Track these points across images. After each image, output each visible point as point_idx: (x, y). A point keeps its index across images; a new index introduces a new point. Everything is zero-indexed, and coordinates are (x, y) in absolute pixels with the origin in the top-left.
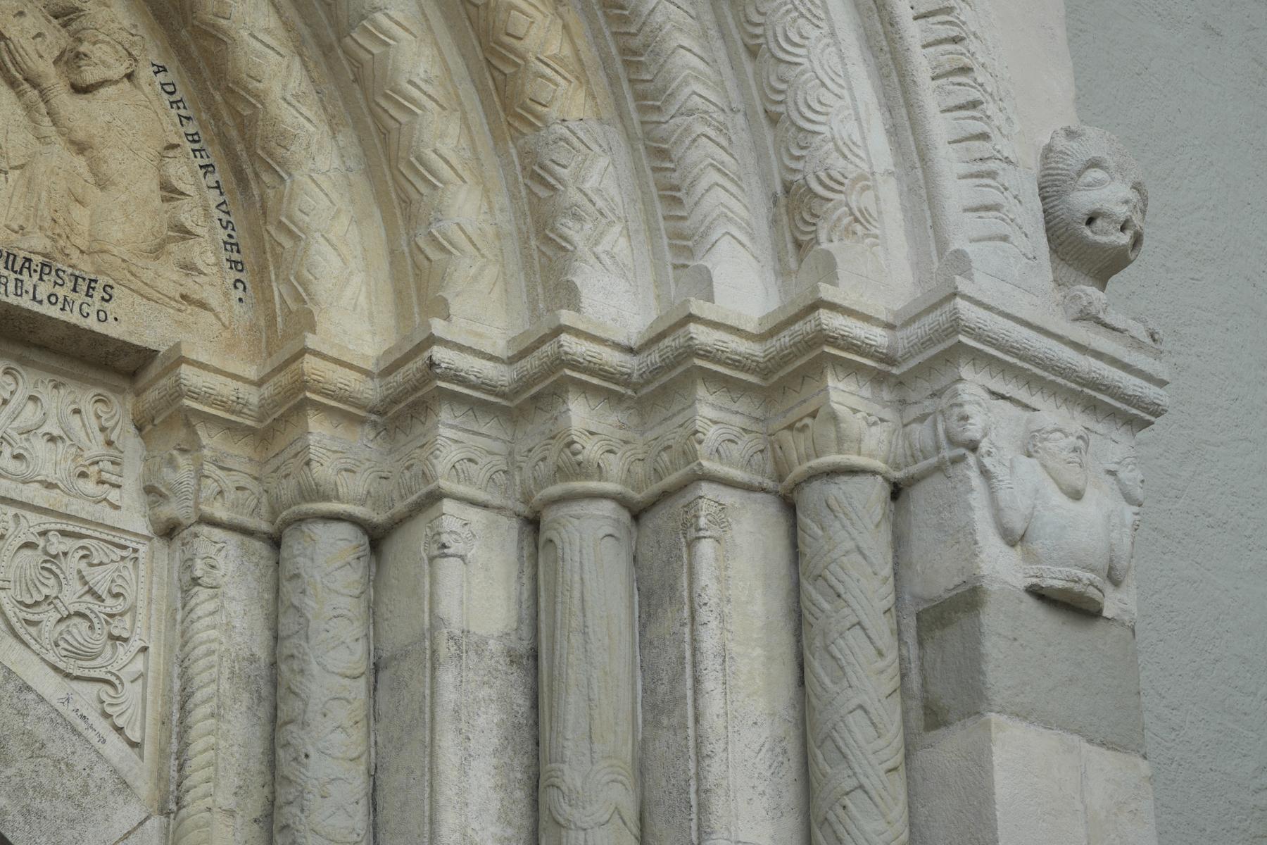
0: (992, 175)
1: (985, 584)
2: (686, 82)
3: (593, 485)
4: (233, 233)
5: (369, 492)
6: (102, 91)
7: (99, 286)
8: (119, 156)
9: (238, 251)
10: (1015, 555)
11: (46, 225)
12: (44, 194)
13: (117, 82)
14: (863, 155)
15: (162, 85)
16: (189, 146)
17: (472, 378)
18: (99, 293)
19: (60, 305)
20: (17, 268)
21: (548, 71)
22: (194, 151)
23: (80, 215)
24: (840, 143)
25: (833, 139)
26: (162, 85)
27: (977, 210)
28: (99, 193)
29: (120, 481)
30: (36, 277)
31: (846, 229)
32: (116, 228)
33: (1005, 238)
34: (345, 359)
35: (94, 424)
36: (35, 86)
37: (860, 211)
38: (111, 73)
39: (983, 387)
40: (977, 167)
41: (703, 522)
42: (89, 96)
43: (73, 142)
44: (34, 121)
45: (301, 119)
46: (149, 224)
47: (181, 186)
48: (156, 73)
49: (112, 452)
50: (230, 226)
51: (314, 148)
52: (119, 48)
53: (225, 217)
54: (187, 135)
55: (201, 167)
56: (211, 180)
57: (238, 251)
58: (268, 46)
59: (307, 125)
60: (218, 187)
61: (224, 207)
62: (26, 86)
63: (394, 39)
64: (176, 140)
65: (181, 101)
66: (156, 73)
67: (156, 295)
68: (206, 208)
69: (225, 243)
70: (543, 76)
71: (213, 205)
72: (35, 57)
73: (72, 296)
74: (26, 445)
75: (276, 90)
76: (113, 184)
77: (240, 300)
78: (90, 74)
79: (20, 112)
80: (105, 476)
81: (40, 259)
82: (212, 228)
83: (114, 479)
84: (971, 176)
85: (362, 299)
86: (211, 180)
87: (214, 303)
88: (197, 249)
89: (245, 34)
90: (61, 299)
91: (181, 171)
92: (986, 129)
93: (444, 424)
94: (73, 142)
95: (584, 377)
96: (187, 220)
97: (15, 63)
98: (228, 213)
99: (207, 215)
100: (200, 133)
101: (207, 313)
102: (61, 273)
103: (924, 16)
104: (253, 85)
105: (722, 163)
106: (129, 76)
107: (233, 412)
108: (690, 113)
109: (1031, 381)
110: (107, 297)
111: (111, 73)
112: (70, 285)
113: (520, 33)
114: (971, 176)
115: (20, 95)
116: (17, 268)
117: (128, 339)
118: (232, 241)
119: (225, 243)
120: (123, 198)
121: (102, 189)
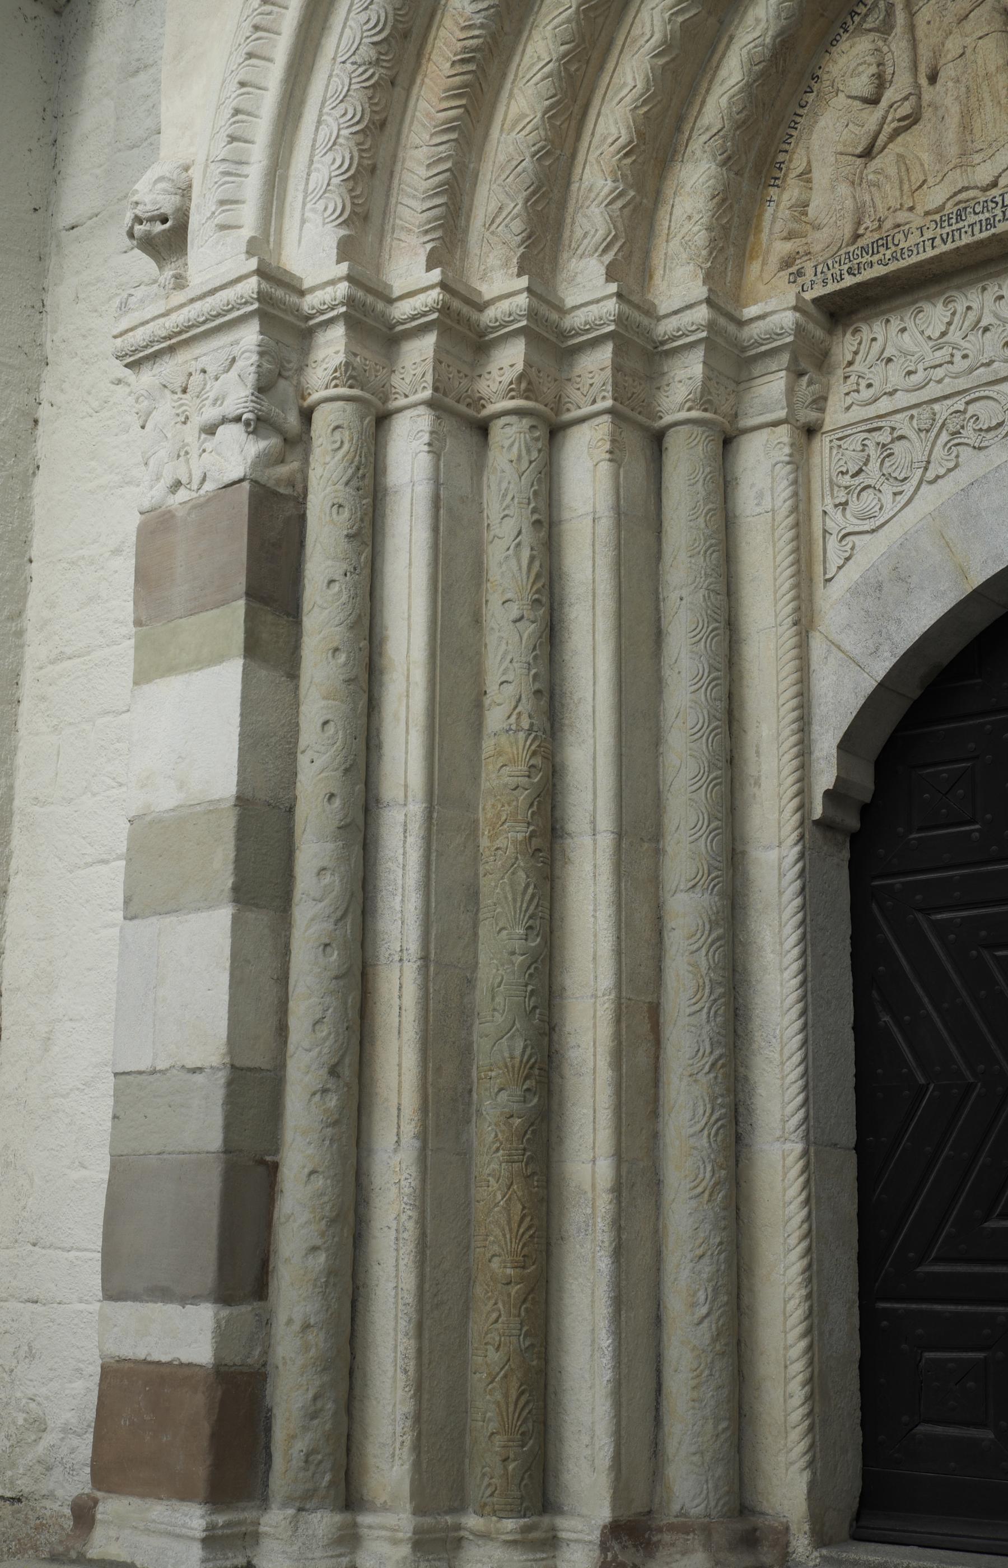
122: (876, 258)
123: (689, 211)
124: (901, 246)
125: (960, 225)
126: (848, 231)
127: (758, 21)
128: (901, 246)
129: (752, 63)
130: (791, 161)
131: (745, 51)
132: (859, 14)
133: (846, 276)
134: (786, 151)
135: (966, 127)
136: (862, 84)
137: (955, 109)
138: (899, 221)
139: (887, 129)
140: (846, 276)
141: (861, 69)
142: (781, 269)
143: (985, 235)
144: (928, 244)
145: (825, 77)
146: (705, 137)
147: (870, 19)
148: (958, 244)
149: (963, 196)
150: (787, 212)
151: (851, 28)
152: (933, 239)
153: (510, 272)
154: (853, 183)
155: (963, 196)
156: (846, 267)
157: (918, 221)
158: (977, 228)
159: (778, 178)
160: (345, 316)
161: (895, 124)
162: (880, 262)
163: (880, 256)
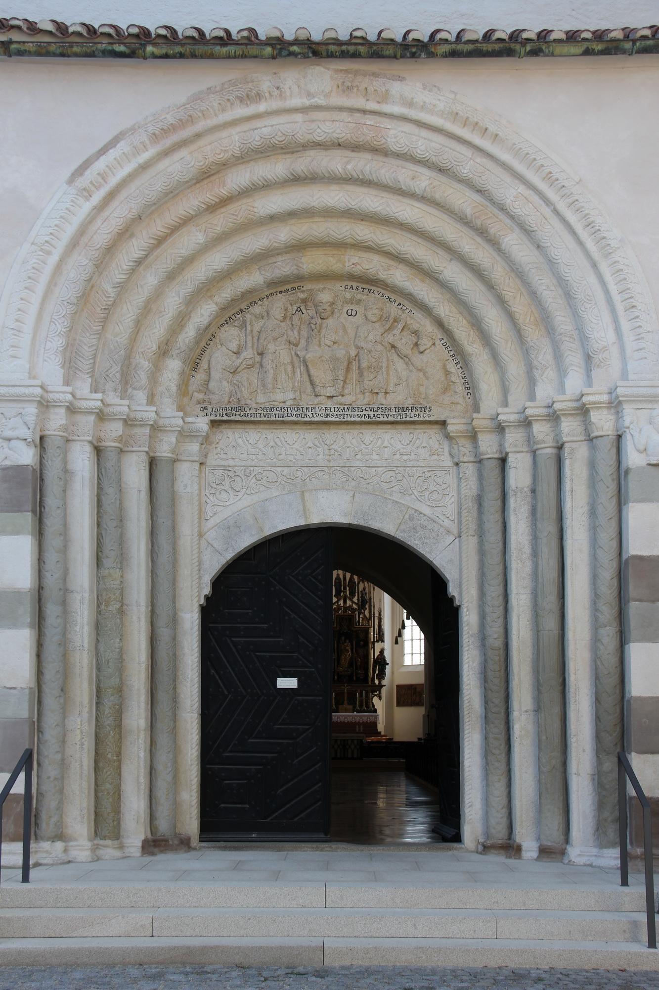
0: (642, 338)
1: (630, 467)
2: (559, 326)
3: (543, 446)
10: (643, 455)
14: (605, 340)
18: (428, 409)
21: (526, 328)
23: (422, 389)
24: (597, 339)
25: (595, 338)
27: (638, 350)
31: (598, 366)
33: (646, 358)
37: (603, 359)
39: (633, 408)
40: (637, 337)
41: (566, 454)
43: (418, 370)
47: (451, 370)
51: (478, 356)
53: (463, 376)
56: (459, 366)
59: (476, 350)
62: (405, 358)
68: (458, 374)
75: (466, 343)
79: (405, 365)
81: (411, 406)
82: (460, 380)
84: (636, 340)
86: (459, 366)
87: (460, 402)
89: (455, 329)
91: (451, 366)
92: (640, 324)
95: (535, 418)
96: (453, 379)
99: (459, 376)
103: (621, 292)
104: (460, 342)
105: (571, 347)
108: (561, 334)
109: (651, 401)
113: (518, 318)
114: (636, 340)
115: (404, 360)
121: (428, 380)
122: (237, 413)
123: (170, 378)
124: (248, 412)
125: (271, 413)
126: (227, 399)
127: (203, 315)
128: (248, 412)
129: (199, 329)
131: (196, 325)
133: (225, 416)
135: (275, 379)
136: (234, 346)
137: (271, 371)
138: (247, 403)
139: (243, 367)
140: (225, 416)
141: (233, 341)
142: (197, 404)
143: (280, 419)
144: (258, 415)
145: (218, 337)
146: (177, 351)
147: (236, 322)
148: (269, 419)
149: (273, 403)
151: (229, 323)
152: (261, 414)
153: (117, 394)
154: (228, 382)
155: (273, 403)
156: (225, 413)
157: (254, 405)
158: (277, 416)
160: (68, 407)
161: (245, 366)
162: (239, 415)
163: (239, 413)
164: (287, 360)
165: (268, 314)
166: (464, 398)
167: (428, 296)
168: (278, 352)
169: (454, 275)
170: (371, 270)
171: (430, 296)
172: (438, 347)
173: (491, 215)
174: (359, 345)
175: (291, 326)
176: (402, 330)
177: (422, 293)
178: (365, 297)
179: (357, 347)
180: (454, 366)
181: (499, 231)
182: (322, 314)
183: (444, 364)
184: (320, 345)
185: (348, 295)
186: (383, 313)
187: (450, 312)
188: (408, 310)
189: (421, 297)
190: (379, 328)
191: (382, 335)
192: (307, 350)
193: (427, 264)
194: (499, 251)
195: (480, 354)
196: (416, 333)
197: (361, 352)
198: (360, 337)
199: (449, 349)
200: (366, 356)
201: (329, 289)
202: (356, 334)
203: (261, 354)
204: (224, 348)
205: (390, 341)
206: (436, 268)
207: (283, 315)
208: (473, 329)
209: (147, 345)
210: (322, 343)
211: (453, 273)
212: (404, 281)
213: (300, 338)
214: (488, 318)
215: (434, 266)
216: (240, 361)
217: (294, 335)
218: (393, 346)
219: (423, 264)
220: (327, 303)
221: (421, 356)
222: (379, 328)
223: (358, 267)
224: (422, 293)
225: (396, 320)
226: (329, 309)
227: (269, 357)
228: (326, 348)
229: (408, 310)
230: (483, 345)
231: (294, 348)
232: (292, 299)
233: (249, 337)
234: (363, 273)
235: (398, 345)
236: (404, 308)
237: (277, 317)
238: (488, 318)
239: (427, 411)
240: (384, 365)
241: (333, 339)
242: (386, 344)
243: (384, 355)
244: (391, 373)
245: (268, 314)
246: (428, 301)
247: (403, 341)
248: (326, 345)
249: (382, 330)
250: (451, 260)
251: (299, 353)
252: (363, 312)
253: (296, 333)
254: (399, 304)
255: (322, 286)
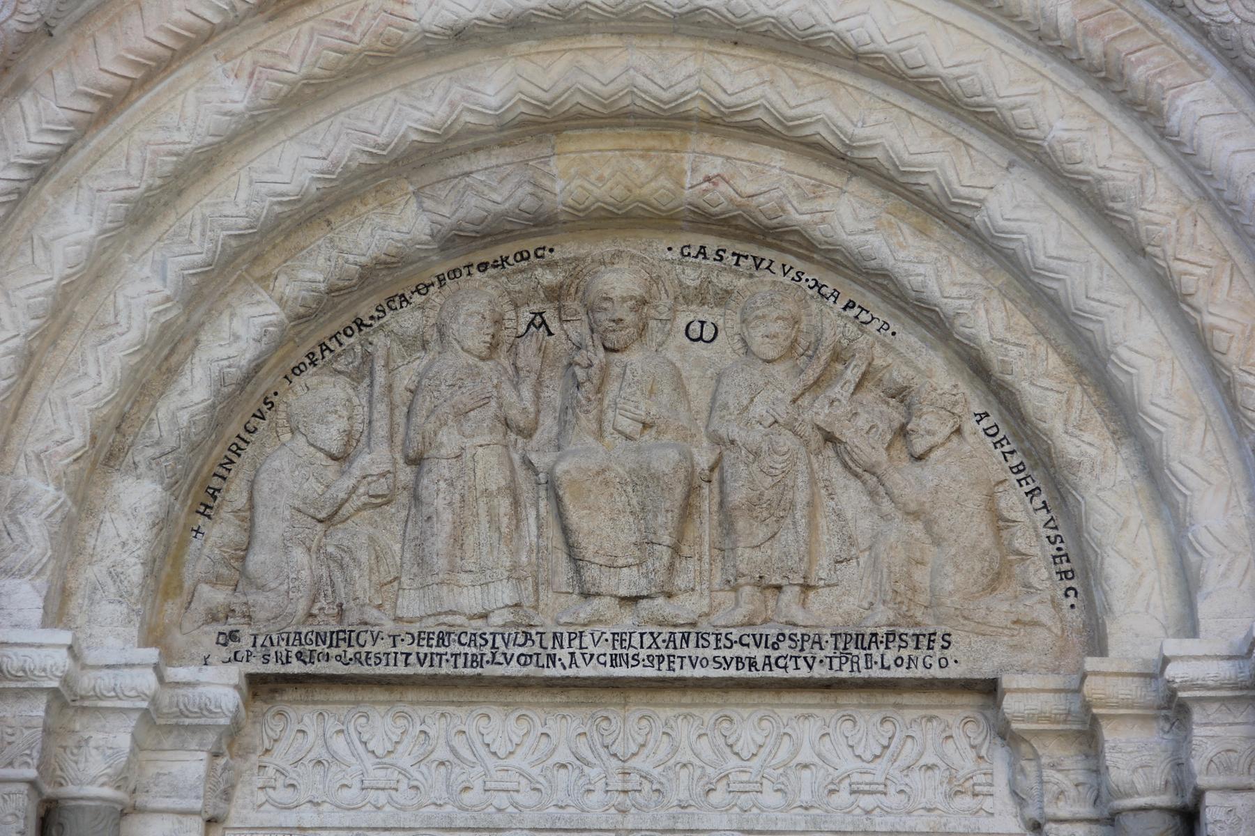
4: (1062, 545)
5: (1167, 782)
6: (932, 455)
7: (938, 638)
8: (947, 514)
9: (1068, 561)
11: (888, 598)
12: (885, 570)
13: (943, 444)
15: (985, 430)
16: (1013, 478)
17: (1210, 683)
18: (939, 643)
19: (905, 665)
20: (866, 645)
22: (1019, 481)
23: (921, 576)
26: (985, 430)
28: (935, 549)
29: (991, 789)
30: (882, 647)
32: (948, 581)
34: (1125, 670)
35: (963, 743)
36: (874, 474)
38: (936, 439)
42: (922, 462)
43: (908, 514)
44: (875, 502)
45: (1085, 447)
46: (978, 567)
47: (1012, 516)
48: (978, 422)
49: (984, 766)
50: (1059, 539)
51: (1097, 470)
52: (943, 412)
53: (1052, 533)
54: (1011, 468)
55: (1027, 494)
56: (1038, 502)
57: (1068, 561)
58: (1047, 389)
60: (1045, 507)
61: (1051, 524)
62: (867, 476)
63: (1133, 367)
64: (1002, 478)
65: (1005, 437)
66: (978, 422)
67: (988, 630)
68: (1035, 529)
69: (1054, 557)
70: (1247, 385)
71: (1040, 525)
72: (869, 450)
73: (915, 653)
74: (907, 780)
75: (1058, 426)
76: (944, 540)
77: (1072, 606)
78: (920, 446)
79: (865, 498)
80: (978, 789)
81: (885, 630)
82: (1043, 546)
83: (985, 789)
85: (1156, 599)
86: (1038, 502)
87: (1044, 619)
88: (1032, 569)
89: (1025, 384)
90: (906, 660)
91: (1013, 501)
93: (1197, 724)
94: (908, 514)
96: (1019, 544)
97: (854, 461)
98: (1056, 528)
99: (1038, 536)
100: (1025, 461)
101: (1038, 630)
102: (904, 637)
104: (1042, 425)
106: (958, 431)
107: (1058, 723)
110: (946, 644)
111: (936, 439)
112: (912, 644)
113: (1223, 349)
115: (864, 483)
116: (866, 645)
117: (968, 676)
118: (1062, 553)
119: (1054, 557)
120: (953, 551)
121: (939, 545)
130: (227, 491)
131: (215, 368)
132: (331, 351)
134: (224, 479)
136: (331, 435)
145: (282, 407)
147: (342, 360)
150: (217, 551)
159: (211, 508)
164: (497, 479)
165: (442, 335)
166: (1055, 604)
167: (938, 277)
168: (467, 455)
169: (1020, 214)
170: (761, 199)
171: (946, 278)
172: (971, 439)
173: (1137, 24)
174: (722, 432)
175: (511, 371)
176: (859, 386)
177: (921, 269)
178: (743, 280)
179: (717, 440)
180: (1022, 502)
181: (1161, 74)
182: (611, 336)
183: (991, 497)
184: (600, 434)
185: (691, 277)
186: (799, 331)
187: (1008, 329)
188: (876, 324)
189: (916, 281)
190: (786, 383)
191: (794, 401)
192: (559, 448)
193: (937, 179)
194: (1163, 136)
195: (1104, 466)
196: (900, 394)
197: (729, 456)
198: (725, 406)
199: (1007, 448)
200: (742, 467)
201: (633, 256)
202: (714, 400)
203: (416, 461)
204: (301, 440)
205: (820, 420)
206: (964, 191)
207: (488, 338)
208: (1081, 384)
209: (52, 432)
210: (608, 428)
211: (1017, 206)
212: (864, 232)
213: (538, 412)
214: (1131, 349)
215: (956, 186)
216: (349, 482)
217: (520, 401)
218: (829, 438)
219: (923, 180)
220: (624, 300)
221: (916, 469)
222: (786, 383)
223: (723, 187)
224: (921, 269)
225: (838, 356)
226: (630, 318)
227: (441, 469)
228: (620, 441)
229: (876, 324)
230: (1114, 433)
231: (521, 441)
232: (518, 288)
233: (381, 408)
234: (739, 206)
235: (847, 434)
236: (864, 317)
237: (469, 344)
238: (1131, 349)
239: (937, 646)
240: (801, 497)
241: (642, 413)
242: (807, 430)
243: (801, 466)
244: (823, 522)
245: (442, 335)
246: (938, 294)
247: (862, 422)
248: (620, 432)
249: (794, 386)
250: (1011, 164)
251: (534, 457)
252: (736, 330)
253: (527, 392)
254: (850, 305)
255: (612, 249)
